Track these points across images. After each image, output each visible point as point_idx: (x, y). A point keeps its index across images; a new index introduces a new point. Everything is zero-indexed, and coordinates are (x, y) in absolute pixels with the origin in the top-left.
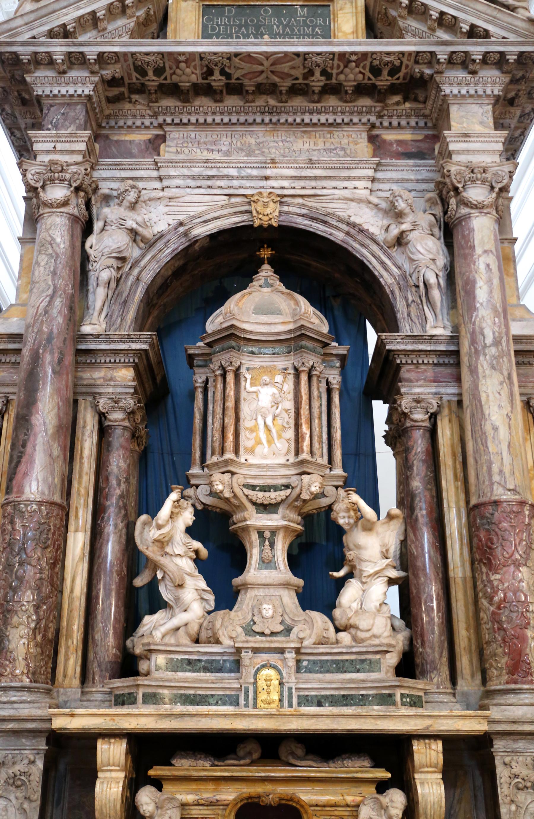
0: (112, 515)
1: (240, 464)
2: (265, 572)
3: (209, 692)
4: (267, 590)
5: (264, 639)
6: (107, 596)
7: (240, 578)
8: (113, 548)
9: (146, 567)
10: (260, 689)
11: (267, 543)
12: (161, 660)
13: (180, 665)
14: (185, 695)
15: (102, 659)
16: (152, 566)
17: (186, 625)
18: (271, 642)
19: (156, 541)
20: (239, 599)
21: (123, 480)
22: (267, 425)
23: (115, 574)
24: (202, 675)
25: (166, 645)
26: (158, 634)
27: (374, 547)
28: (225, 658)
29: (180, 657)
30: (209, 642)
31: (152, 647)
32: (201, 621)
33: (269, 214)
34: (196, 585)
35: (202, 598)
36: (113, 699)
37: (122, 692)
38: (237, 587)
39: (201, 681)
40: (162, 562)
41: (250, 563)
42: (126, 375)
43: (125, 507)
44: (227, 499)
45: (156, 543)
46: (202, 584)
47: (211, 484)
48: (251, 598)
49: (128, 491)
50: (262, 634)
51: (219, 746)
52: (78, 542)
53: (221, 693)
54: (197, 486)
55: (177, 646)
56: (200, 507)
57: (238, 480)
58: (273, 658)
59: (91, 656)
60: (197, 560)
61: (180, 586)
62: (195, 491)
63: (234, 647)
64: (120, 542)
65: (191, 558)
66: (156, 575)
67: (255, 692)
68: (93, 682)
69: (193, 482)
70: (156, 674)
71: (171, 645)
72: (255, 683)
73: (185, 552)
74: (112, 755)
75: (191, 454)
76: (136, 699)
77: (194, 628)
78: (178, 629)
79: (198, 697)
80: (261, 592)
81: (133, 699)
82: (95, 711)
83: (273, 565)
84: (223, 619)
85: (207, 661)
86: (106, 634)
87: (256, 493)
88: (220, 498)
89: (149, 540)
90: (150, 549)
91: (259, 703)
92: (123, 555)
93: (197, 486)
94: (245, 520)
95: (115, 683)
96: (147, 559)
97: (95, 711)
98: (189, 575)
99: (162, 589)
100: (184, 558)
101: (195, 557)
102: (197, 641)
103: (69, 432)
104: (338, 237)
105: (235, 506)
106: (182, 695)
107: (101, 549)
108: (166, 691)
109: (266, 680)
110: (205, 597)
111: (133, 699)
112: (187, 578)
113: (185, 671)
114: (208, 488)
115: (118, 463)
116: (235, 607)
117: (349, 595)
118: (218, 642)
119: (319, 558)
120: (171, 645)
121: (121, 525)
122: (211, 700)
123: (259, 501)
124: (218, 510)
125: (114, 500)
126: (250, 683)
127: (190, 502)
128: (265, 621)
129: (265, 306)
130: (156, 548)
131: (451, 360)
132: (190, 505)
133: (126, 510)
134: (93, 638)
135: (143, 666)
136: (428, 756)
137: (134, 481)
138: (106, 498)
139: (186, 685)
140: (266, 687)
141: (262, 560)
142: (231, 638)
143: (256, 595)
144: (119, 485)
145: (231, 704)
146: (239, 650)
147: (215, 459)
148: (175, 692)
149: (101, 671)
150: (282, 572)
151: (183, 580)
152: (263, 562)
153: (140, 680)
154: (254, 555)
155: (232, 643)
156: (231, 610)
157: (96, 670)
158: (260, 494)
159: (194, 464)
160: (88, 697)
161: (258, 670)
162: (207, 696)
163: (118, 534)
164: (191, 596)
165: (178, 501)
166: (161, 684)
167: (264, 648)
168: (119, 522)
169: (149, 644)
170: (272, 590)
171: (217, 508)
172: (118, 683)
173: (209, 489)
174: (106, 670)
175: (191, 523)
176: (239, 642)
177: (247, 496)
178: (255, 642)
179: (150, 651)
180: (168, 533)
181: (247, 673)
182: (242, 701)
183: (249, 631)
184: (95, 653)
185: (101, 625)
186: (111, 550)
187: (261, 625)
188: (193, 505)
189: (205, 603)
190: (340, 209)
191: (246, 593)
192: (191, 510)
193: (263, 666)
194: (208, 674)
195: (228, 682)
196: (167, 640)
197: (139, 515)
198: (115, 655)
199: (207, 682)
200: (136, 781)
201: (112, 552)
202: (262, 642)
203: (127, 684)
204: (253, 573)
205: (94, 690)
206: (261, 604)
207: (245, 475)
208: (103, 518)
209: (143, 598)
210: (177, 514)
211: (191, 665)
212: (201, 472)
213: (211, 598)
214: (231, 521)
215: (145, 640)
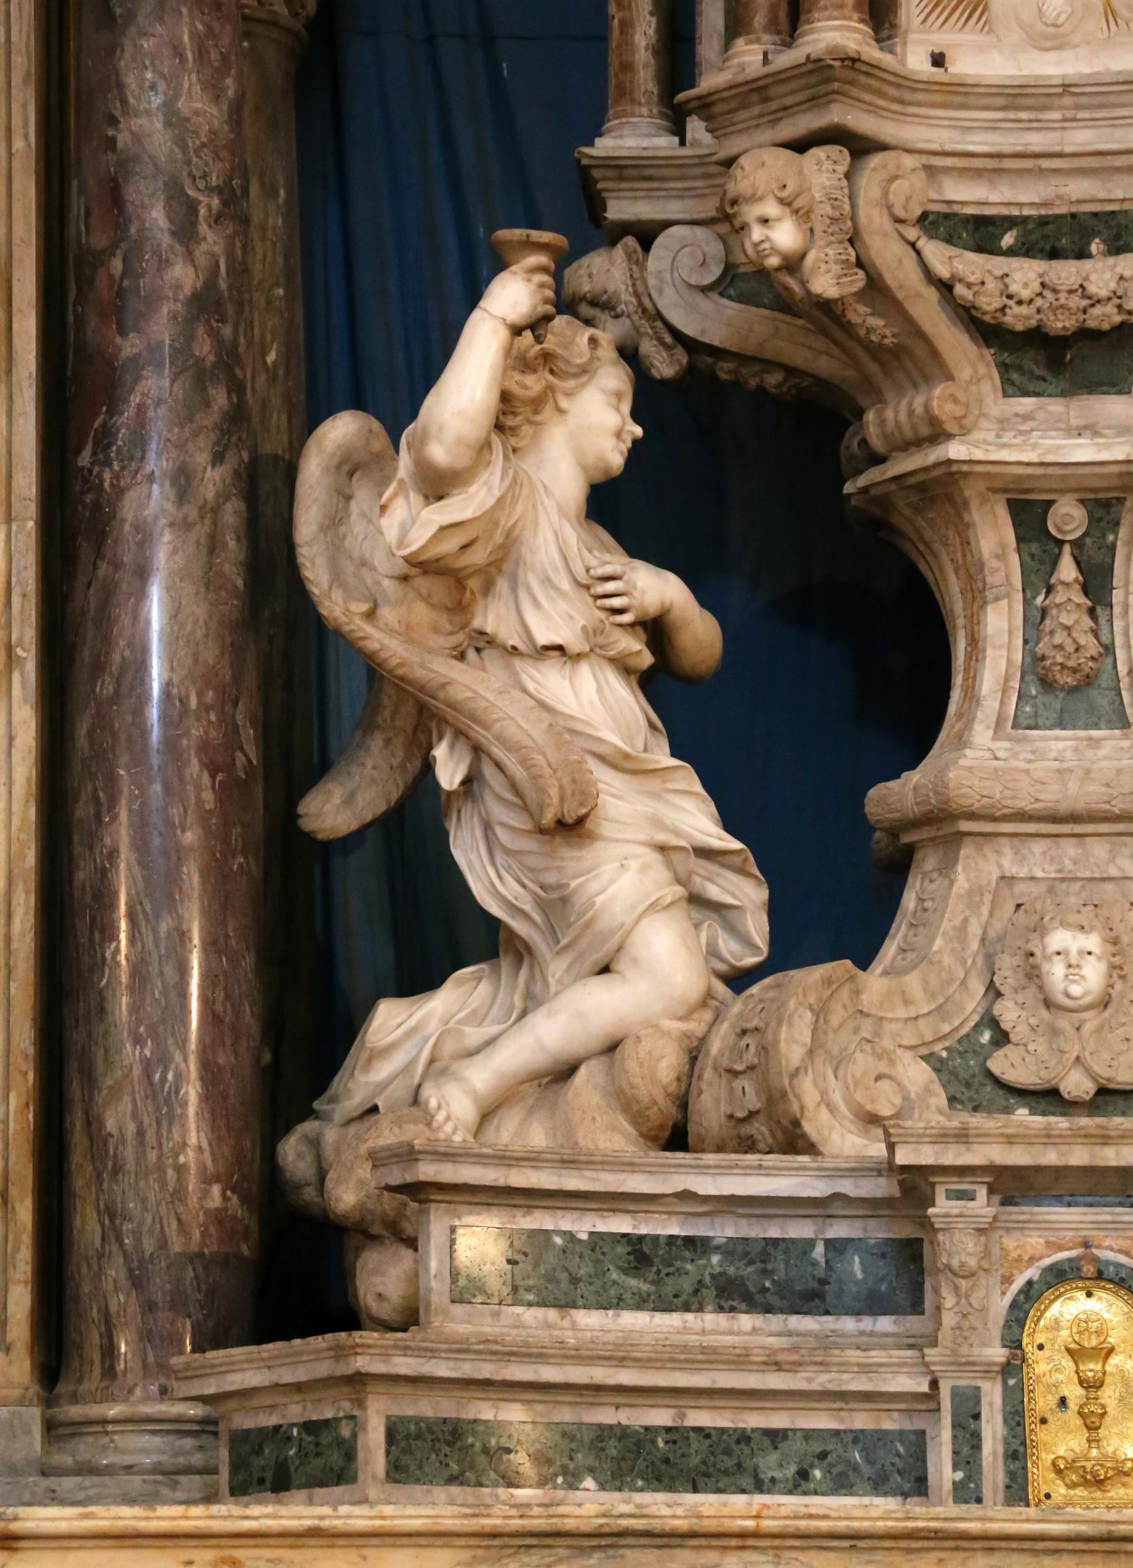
0: (160, 425)
1: (901, 90)
2: (1059, 744)
3: (755, 1420)
4: (1070, 848)
5: (1061, 1123)
6: (161, 891)
7: (913, 778)
8: (174, 615)
9: (367, 725)
10: (1043, 1402)
11: (1067, 570)
12: (478, 1242)
13: (584, 1270)
14: (622, 1433)
15: (149, 1245)
16: (406, 720)
17: (612, 1048)
18: (1105, 1139)
19: (422, 567)
20: (909, 900)
21: (209, 204)
23: (194, 766)
24: (709, 1325)
25: (504, 1159)
26: (454, 1105)
28: (839, 1230)
29: (584, 1225)
30: (748, 1145)
31: (427, 1171)
32: (695, 1027)
34: (657, 822)
35: (696, 900)
36: (224, 1454)
37: (272, 1420)
38: (894, 831)
39: (710, 1357)
40: (459, 694)
41: (971, 695)
43: (229, 365)
44: (825, 306)
45: (423, 584)
46: (697, 819)
47: (726, 220)
48: (974, 896)
49: (240, 271)
50: (1048, 1098)
53: (823, 1421)
54: (646, 235)
55: (569, 1162)
56: (664, 365)
57: (891, 189)
58: (1117, 1227)
59: (87, 1226)
60: (662, 681)
61: (572, 828)
62: (637, 263)
63: (889, 1168)
64: (211, 581)
65: (623, 666)
66: (428, 766)
67: (1016, 1416)
68: (109, 1372)
69: (618, 209)
70: (459, 1322)
71: (533, 1159)
72: (1013, 1369)
73: (591, 633)
75: (601, 38)
76: (350, 1455)
77: (657, 1066)
78: (563, 1072)
79: (697, 1445)
80: (1036, 861)
81: (334, 1458)
82: (128, 1517)
83: (1102, 701)
84: (820, 1013)
85: (735, 1249)
86: (165, 1105)
87: (999, 264)
88: (785, 304)
89: (381, 563)
90: (387, 614)
91: (1041, 1477)
92: (237, 652)
93: (646, 235)
94: (938, 435)
95: (231, 1367)
96: (374, 672)
97: (128, 1517)
98: (622, 763)
99: (468, 851)
100: (585, 670)
101: (647, 659)
102: (676, 1138)
105: (876, 351)
106: (603, 1432)
107: (104, 620)
108: (514, 1413)
109: (1076, 1354)
110: (714, 892)
111: (334, 1458)
112: (604, 777)
113: (619, 1304)
114: (707, 242)
116: (890, 949)
118: (793, 1141)
120: (533, 1159)
121: (213, 480)
122: (769, 1463)
123: (1018, 318)
124: (773, 379)
125: (161, 327)
126: (986, 1370)
127: (608, 334)
128: (1064, 1023)
130: (421, 613)
132: (607, 352)
133: (236, 388)
134: (93, 1124)
135: (380, 1279)
137: (271, 215)
138: (120, 311)
139: (627, 1377)
140: (1074, 1393)
141: (1039, 674)
142: (872, 1120)
143: (1006, 880)
144: (185, 231)
145: (879, 1485)
146: (915, 1186)
147: (750, 57)
148: (566, 1415)
149: (150, 1307)
151: (586, 793)
152: (1047, 684)
153: (372, 1352)
154: (994, 646)
155: (878, 1150)
156: (864, 962)
157: (122, 1301)
158: (1025, 275)
159: (625, 93)
160: (84, 1449)
161: (1028, 1301)
162: (744, 1437)
163: (201, 531)
164: (644, 897)
165: (537, 325)
166: (487, 1370)
167: (1059, 1172)
168: (202, 458)
169: (409, 1154)
170: (1099, 849)
171: (769, 364)
172: (247, 1368)
173: (715, 249)
174: (178, 1303)
175: (616, 460)
176: (919, 1138)
177: (945, 287)
178: (1010, 1140)
179: (419, 1191)
180: (490, 517)
181: (969, 1312)
182: (943, 1469)
183: (971, 1078)
184: (111, 1214)
185: (131, 1055)
186: (163, 624)
187: (1040, 1046)
188: (629, 354)
189: (711, 928)
191: (947, 867)
192: (613, 378)
193: (1059, 1277)
194: (746, 1321)
195: (867, 1360)
196: (506, 1132)
197: (313, 420)
198: (219, 1217)
199: (740, 1360)
201: (171, 640)
202: (1049, 1138)
203: (300, 1374)
205: (114, 1411)
206: (1040, 929)
207: (932, 153)
208: (106, 435)
209: (359, 896)
210: (537, 403)
211: (650, 1268)
212: (664, 143)
213: (749, 895)
214: (851, 443)
215: (385, 1135)
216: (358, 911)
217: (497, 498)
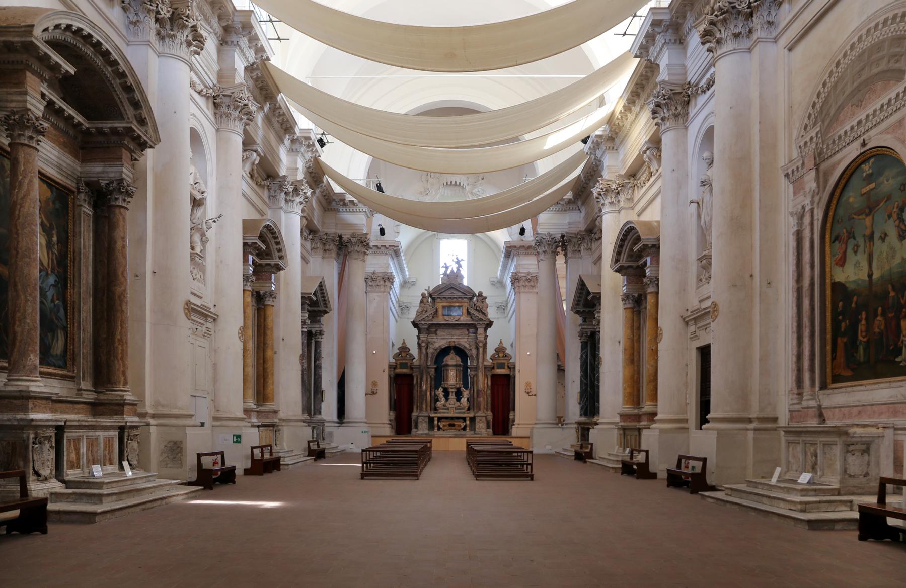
22: (452, 378)
27: (466, 394)
33: (453, 344)
51: (447, 418)
129: (452, 359)
131: (476, 368)
150: (454, 397)
164: (443, 400)
216: (437, 400)
217: (440, 392)
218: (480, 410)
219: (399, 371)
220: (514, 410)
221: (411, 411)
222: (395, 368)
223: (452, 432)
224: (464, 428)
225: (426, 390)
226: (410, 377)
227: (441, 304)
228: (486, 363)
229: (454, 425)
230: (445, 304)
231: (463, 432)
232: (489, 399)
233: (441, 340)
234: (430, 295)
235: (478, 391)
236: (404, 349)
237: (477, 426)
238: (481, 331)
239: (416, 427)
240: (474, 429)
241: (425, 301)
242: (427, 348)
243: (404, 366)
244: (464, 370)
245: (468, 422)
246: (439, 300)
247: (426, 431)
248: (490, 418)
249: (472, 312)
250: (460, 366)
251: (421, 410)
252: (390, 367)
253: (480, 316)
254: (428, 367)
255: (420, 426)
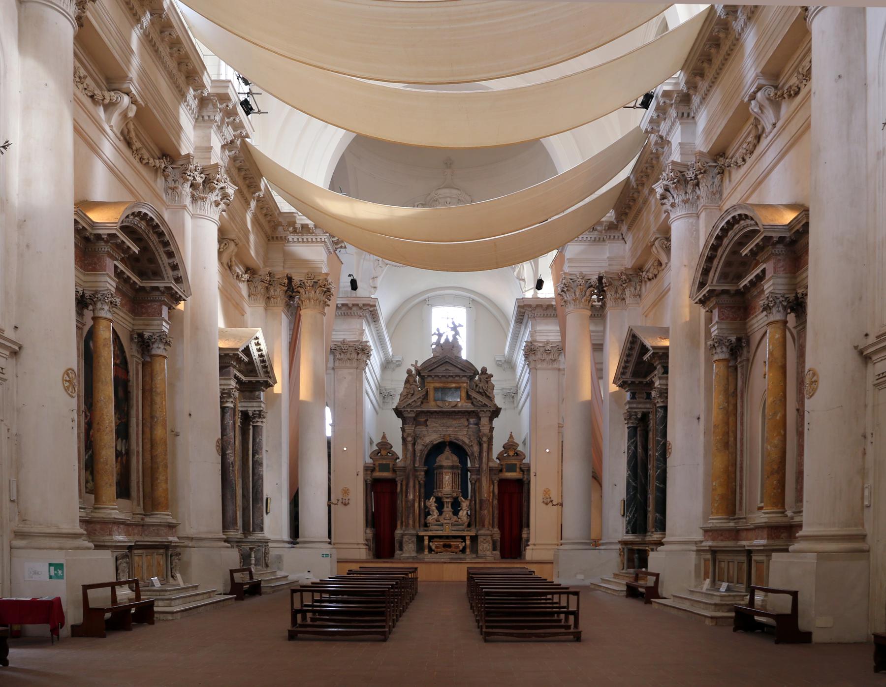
22: (447, 484)
27: (465, 504)
33: (448, 439)
42: (423, 473)
51: (440, 537)
52: (417, 505)
74: (426, 538)
103: (414, 487)
104: (461, 443)
115: (423, 490)
117: (460, 513)
119: (456, 507)
129: (447, 459)
131: (479, 471)
136: (468, 538)
150: (450, 509)
164: (435, 513)
190: (461, 438)
200: (430, 541)
204: (445, 509)
216: (428, 514)
218: (483, 526)
219: (377, 474)
220: (528, 526)
221: (395, 528)
222: (373, 470)
223: (445, 556)
224: (463, 550)
225: (414, 500)
226: (392, 482)
227: (432, 385)
228: (491, 464)
229: (449, 546)
230: (437, 385)
231: (462, 556)
232: (496, 512)
233: (432, 435)
234: (419, 372)
235: (481, 500)
236: (384, 445)
237: (480, 548)
238: (484, 421)
239: (401, 549)
240: (477, 552)
241: (411, 380)
242: (414, 444)
243: (384, 468)
244: (463, 473)
245: (468, 542)
246: (430, 379)
247: (414, 554)
248: (497, 537)
249: (474, 394)
250: (457, 467)
251: (407, 525)
252: (366, 469)
253: (485, 401)
254: (415, 470)
255: (405, 548)
